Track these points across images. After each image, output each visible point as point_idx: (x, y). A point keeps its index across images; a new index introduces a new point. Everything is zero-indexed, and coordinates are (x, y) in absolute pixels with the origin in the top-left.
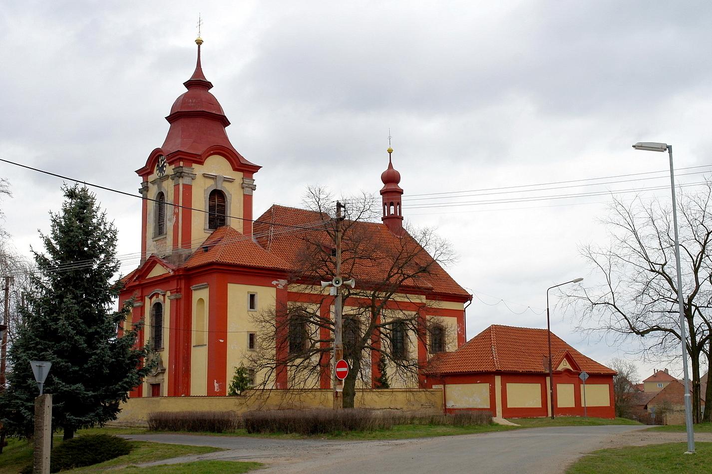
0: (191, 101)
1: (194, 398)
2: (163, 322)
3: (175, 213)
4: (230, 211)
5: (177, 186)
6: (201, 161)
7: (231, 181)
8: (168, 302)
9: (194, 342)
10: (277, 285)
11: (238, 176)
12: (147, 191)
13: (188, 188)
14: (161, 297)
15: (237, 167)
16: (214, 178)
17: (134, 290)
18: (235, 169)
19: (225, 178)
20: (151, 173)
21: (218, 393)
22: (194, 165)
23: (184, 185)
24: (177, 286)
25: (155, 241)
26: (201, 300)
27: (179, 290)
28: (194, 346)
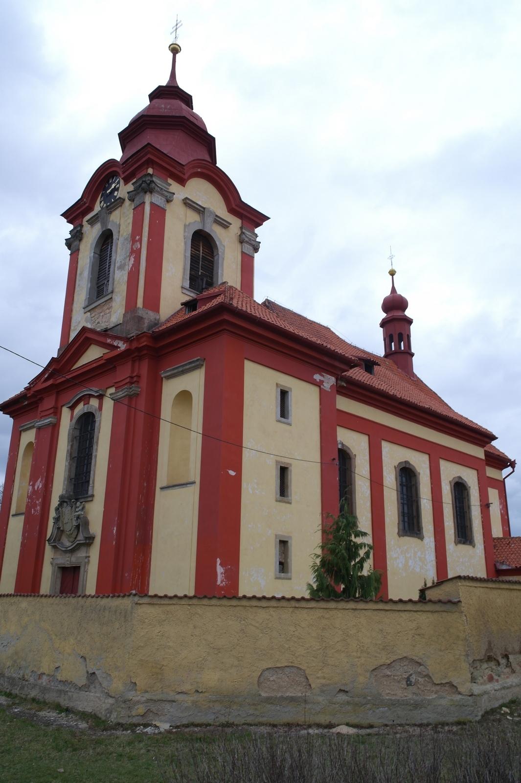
0: (163, 106)
1: (264, 603)
2: (95, 447)
3: (132, 252)
4: (223, 271)
5: (139, 210)
6: (182, 176)
7: (225, 225)
8: (108, 404)
9: (162, 477)
10: (322, 382)
11: (236, 223)
12: (81, 240)
13: (159, 214)
14: (94, 403)
15: (234, 206)
16: (200, 210)
17: (41, 399)
18: (232, 211)
19: (216, 216)
20: (90, 209)
21: (222, 588)
22: (170, 181)
23: (152, 204)
24: (133, 372)
25: (89, 311)
26: (185, 396)
27: (135, 379)
28: (162, 488)
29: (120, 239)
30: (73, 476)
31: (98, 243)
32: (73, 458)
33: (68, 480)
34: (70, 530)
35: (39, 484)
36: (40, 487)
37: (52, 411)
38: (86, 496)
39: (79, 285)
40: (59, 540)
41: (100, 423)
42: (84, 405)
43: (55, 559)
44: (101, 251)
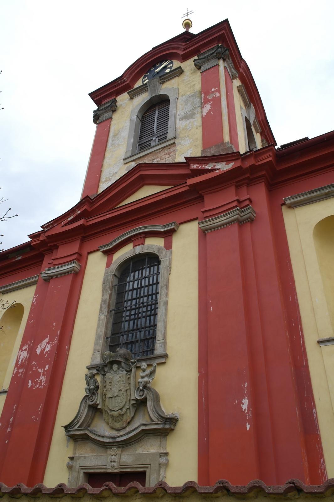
30: (109, 334)
31: (142, 108)
32: (111, 311)
33: (104, 339)
34: (120, 409)
35: (45, 346)
36: (47, 349)
37: (75, 257)
38: (152, 356)
39: (112, 144)
40: (89, 426)
41: (170, 264)
42: (134, 246)
43: (79, 458)
44: (143, 117)
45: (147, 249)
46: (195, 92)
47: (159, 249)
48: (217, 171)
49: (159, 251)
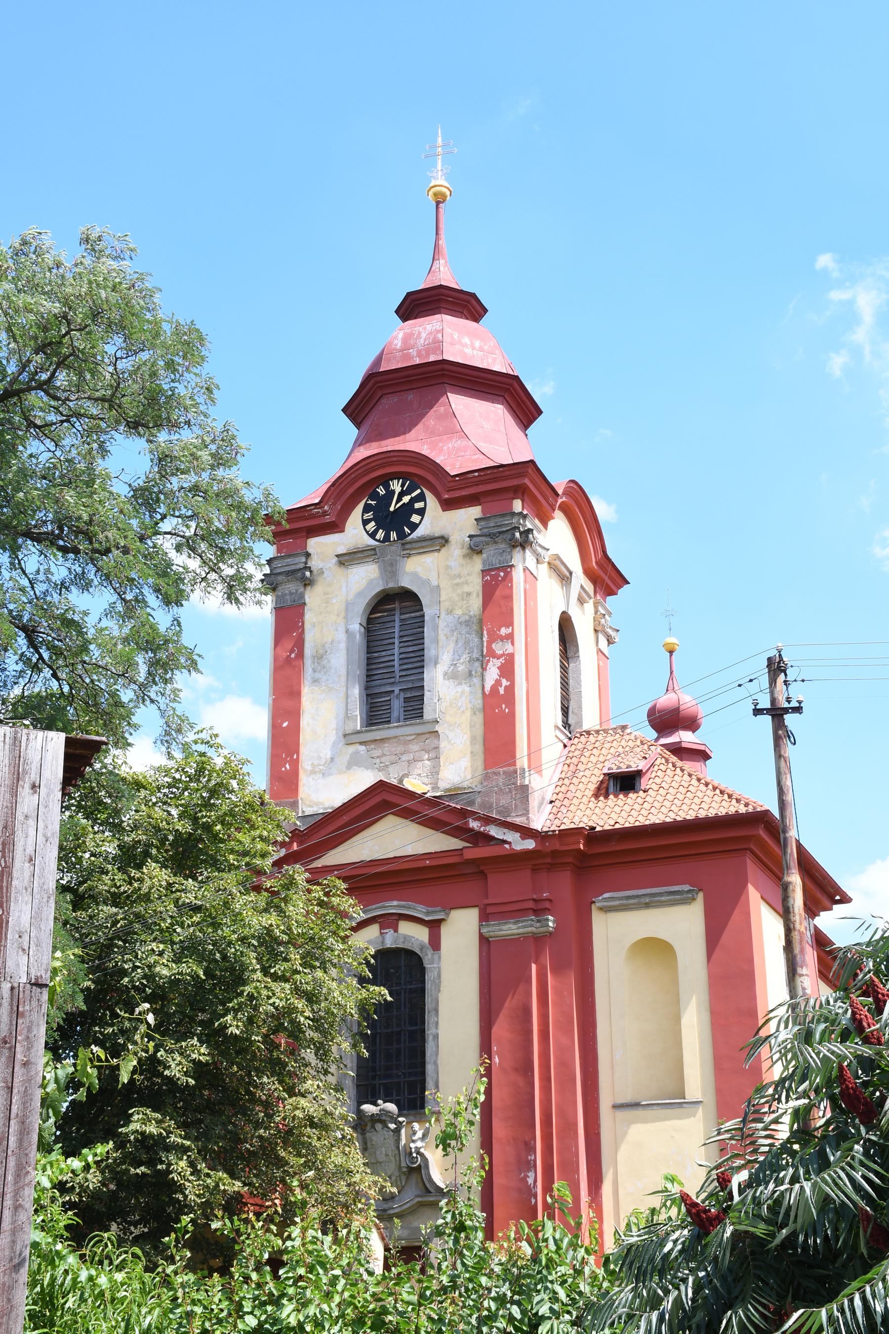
29: (442, 617)
44: (370, 621)
45: (404, 943)
46: (471, 617)
47: (422, 947)
48: (507, 846)
49: (421, 950)
